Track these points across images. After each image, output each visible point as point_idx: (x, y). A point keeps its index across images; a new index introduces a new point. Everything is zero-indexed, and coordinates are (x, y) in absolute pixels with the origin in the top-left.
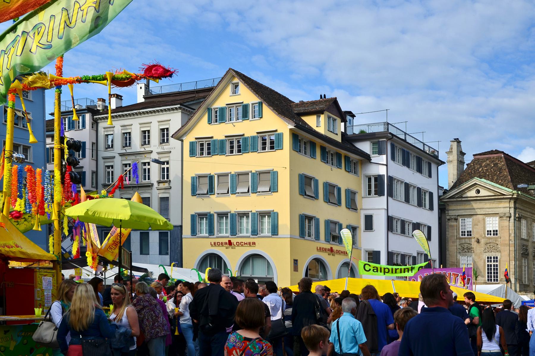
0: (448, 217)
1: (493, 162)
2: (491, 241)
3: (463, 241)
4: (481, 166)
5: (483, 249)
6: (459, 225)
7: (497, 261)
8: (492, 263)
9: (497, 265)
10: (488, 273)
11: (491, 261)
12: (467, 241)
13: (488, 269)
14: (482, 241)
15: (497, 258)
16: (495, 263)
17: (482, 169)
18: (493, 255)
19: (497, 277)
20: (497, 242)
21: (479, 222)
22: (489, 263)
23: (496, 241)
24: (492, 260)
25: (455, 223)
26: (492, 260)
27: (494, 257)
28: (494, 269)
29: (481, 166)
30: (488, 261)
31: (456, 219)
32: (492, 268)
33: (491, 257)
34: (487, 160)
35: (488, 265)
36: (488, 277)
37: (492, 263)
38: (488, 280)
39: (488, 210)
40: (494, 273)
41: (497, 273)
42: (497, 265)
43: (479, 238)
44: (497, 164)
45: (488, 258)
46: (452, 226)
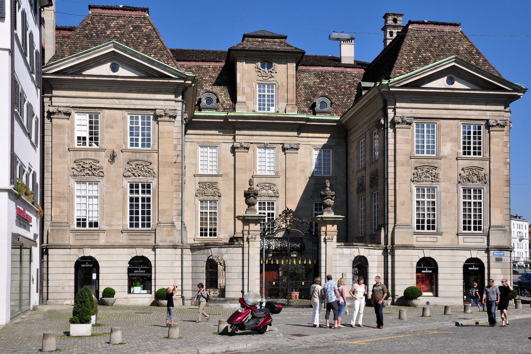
0: (52, 109)
1: (130, 22)
2: (138, 156)
3: (82, 155)
4: (109, 27)
5: (122, 170)
6: (73, 123)
7: (149, 192)
8: (140, 195)
9: (149, 199)
10: (131, 213)
11: (137, 192)
12: (91, 155)
13: (131, 206)
14: (121, 158)
15: (149, 186)
16: (146, 196)
17: (113, 32)
18: (141, 180)
19: (149, 219)
20: (150, 160)
21: (115, 121)
22: (135, 195)
23: (148, 156)
24: (140, 189)
25: (66, 121)
26: (140, 189)
27: (143, 186)
28: (143, 206)
29: (109, 27)
30: (131, 192)
31: (68, 114)
32: (140, 203)
33: (137, 186)
34: (118, 17)
35: (131, 199)
36: (131, 219)
37: (140, 195)
38: (131, 225)
39: (134, 102)
40: (137, 213)
41: (149, 213)
42: (149, 199)
43: (117, 151)
44: (140, 27)
45: (131, 186)
46: (60, 126)
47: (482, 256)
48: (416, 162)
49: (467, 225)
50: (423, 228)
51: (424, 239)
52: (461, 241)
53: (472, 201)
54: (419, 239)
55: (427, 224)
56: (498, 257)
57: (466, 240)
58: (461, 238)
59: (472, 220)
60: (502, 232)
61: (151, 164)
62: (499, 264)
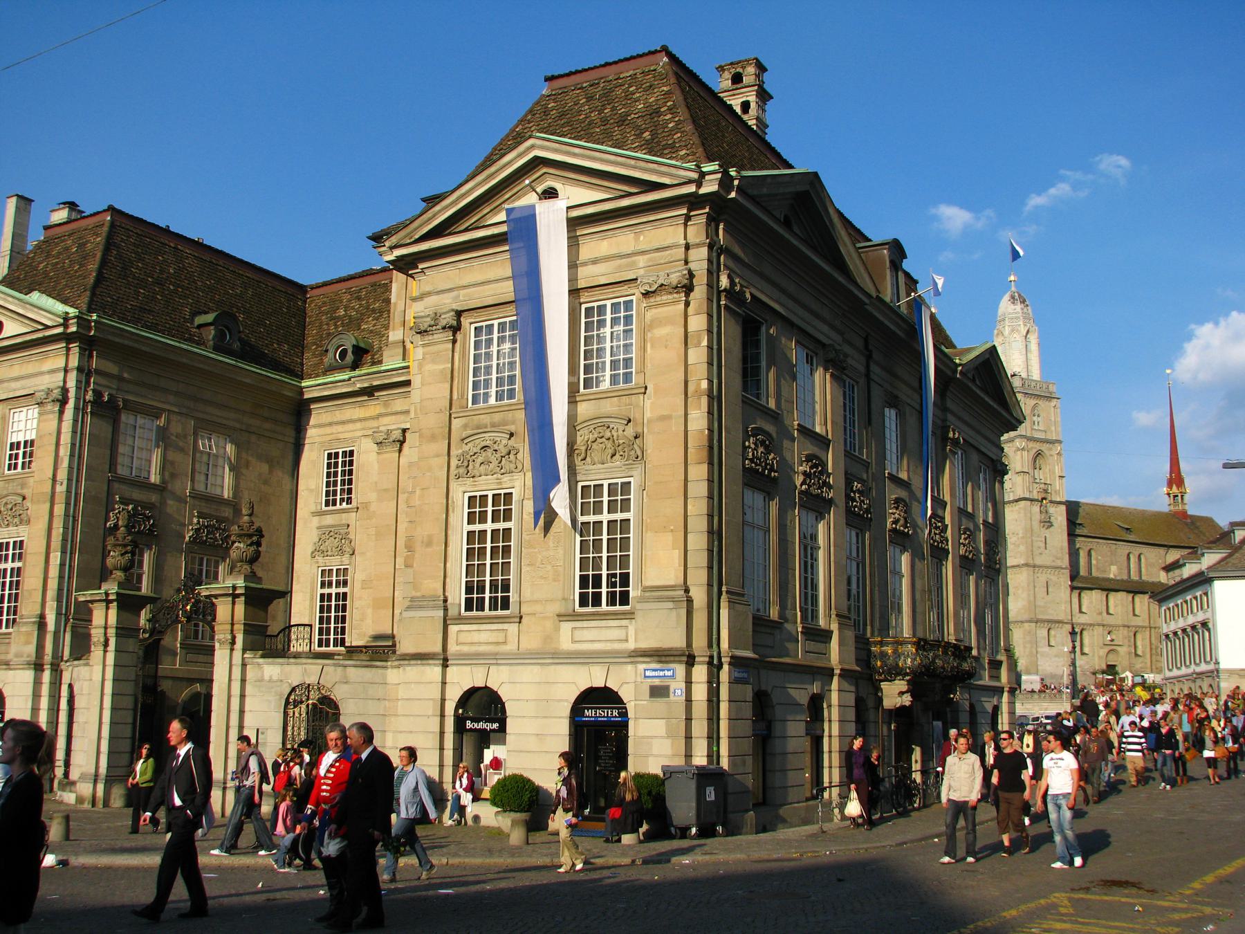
20: (25, 492)
39: (13, 385)
47: (629, 683)
48: (465, 426)
49: (591, 590)
50: (481, 607)
51: (476, 637)
52: (567, 637)
53: (605, 517)
54: (463, 638)
55: (489, 596)
56: (657, 682)
57: (579, 635)
58: (566, 627)
59: (604, 573)
60: (671, 605)
61: (24, 498)
62: (660, 703)
